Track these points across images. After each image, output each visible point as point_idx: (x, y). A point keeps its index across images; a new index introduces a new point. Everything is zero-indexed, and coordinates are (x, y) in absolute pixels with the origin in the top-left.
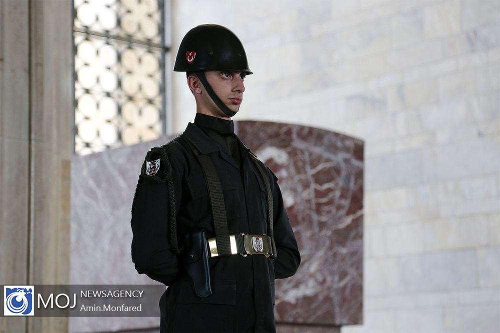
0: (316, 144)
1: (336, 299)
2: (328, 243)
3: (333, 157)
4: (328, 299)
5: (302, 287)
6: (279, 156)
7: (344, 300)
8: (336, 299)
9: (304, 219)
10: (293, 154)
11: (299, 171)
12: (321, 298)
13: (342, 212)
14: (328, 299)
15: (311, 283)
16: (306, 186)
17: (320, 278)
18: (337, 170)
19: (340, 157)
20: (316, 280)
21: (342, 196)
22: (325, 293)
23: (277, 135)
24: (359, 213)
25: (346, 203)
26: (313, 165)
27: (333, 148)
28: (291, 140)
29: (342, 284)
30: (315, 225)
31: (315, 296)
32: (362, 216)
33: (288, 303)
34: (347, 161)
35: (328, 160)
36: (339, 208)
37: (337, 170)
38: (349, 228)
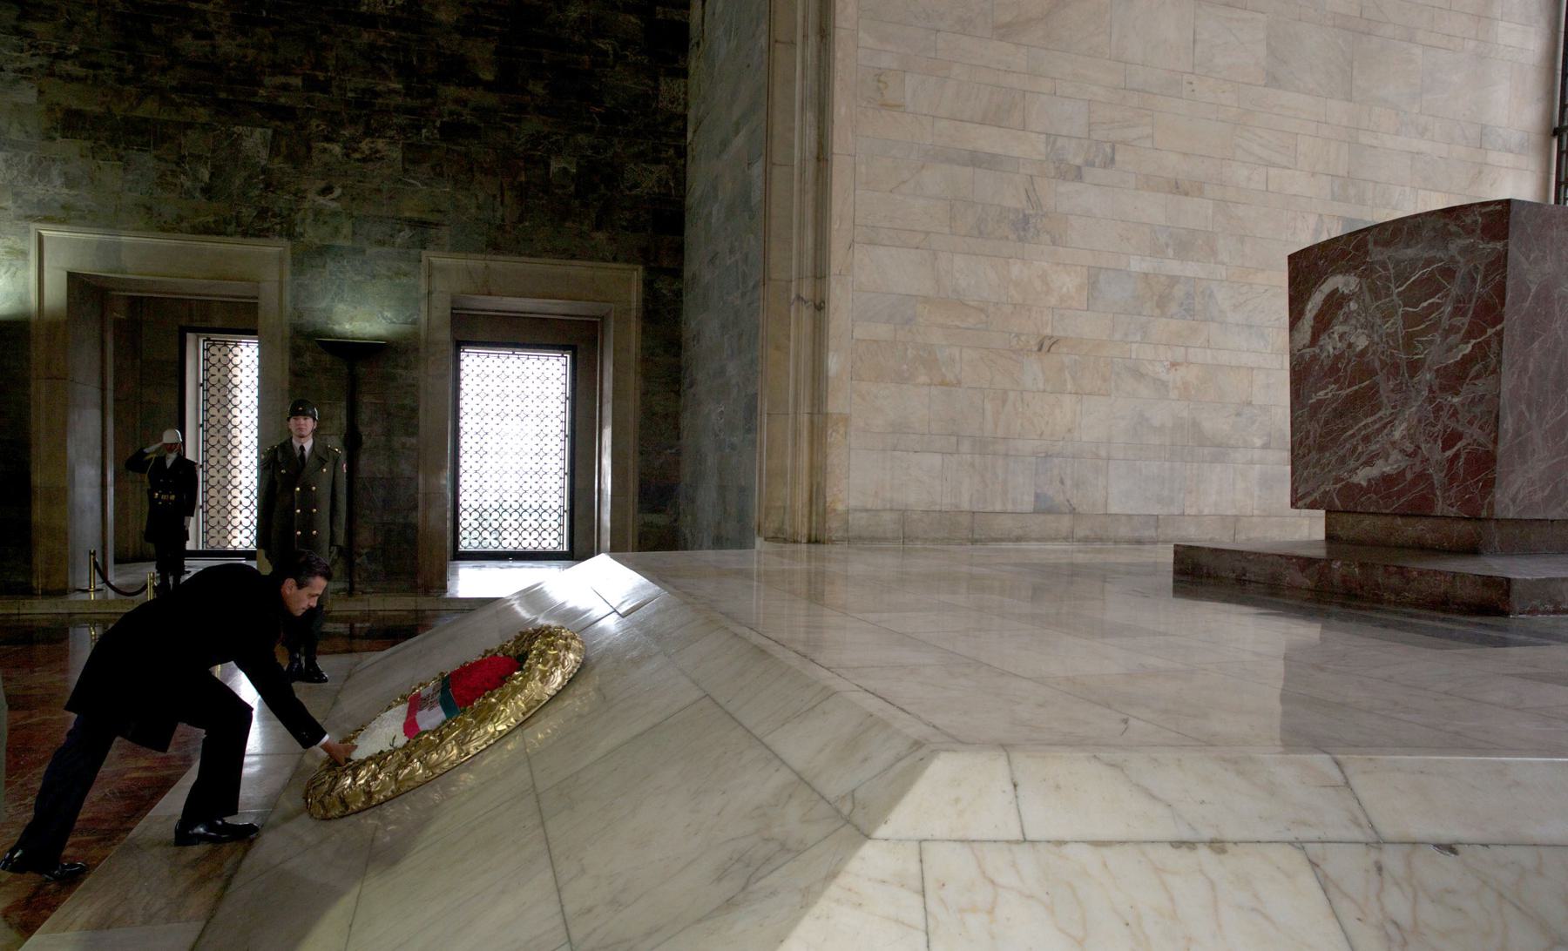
0: (1408, 246)
1: (1438, 477)
2: (1425, 393)
3: (1440, 254)
4: (1422, 476)
5: (1380, 462)
6: (1346, 284)
7: (1452, 478)
8: (1438, 477)
9: (1384, 364)
10: (1367, 273)
11: (1376, 294)
12: (1409, 476)
13: (1453, 339)
14: (1422, 476)
15: (1395, 455)
16: (1387, 315)
17: (1410, 448)
18: (1449, 273)
19: (1454, 248)
20: (1402, 451)
21: (1458, 311)
22: (1418, 469)
23: (1344, 254)
24: (1490, 331)
25: (1464, 322)
26: (1401, 277)
27: (1444, 236)
28: (1367, 253)
29: (1449, 453)
30: (1404, 368)
31: (1402, 474)
32: (1499, 334)
33: (1358, 485)
34: (1464, 251)
35: (1428, 262)
36: (1452, 330)
37: (1449, 273)
38: (1467, 361)
